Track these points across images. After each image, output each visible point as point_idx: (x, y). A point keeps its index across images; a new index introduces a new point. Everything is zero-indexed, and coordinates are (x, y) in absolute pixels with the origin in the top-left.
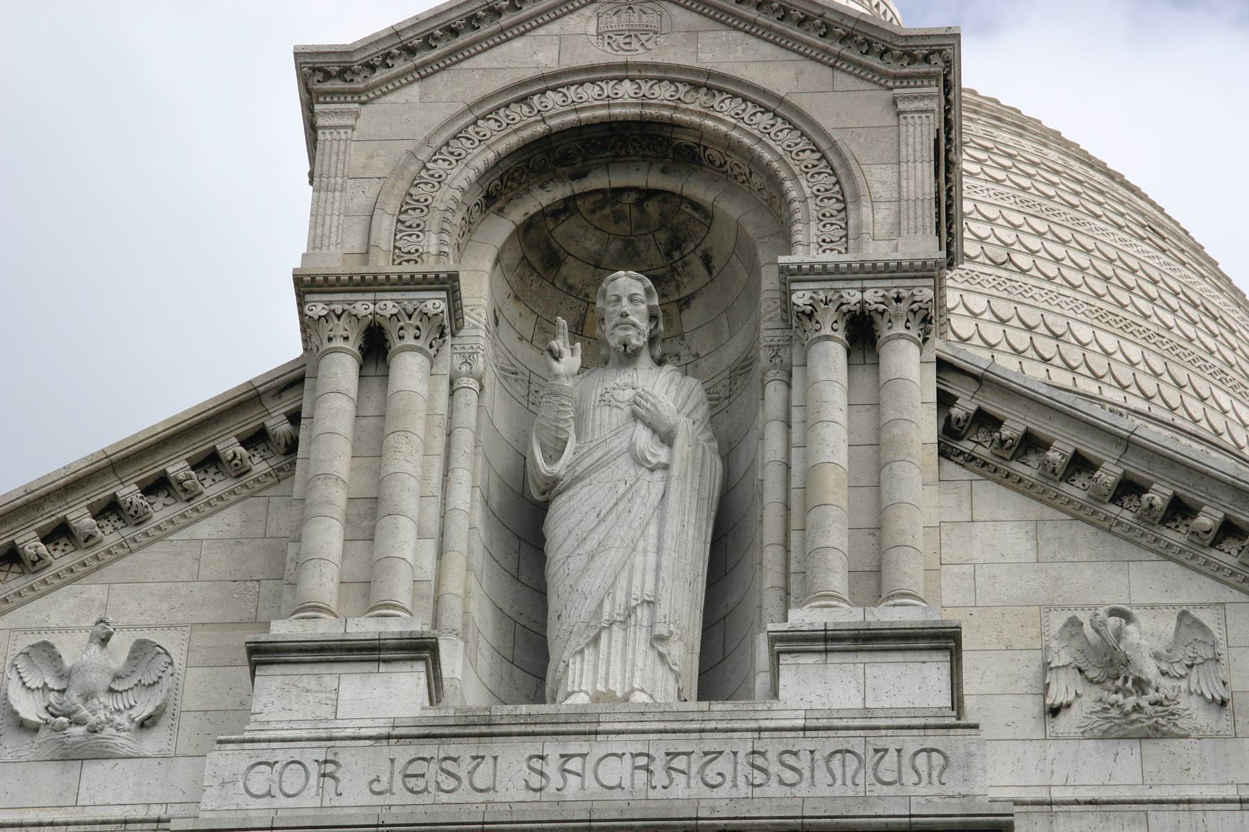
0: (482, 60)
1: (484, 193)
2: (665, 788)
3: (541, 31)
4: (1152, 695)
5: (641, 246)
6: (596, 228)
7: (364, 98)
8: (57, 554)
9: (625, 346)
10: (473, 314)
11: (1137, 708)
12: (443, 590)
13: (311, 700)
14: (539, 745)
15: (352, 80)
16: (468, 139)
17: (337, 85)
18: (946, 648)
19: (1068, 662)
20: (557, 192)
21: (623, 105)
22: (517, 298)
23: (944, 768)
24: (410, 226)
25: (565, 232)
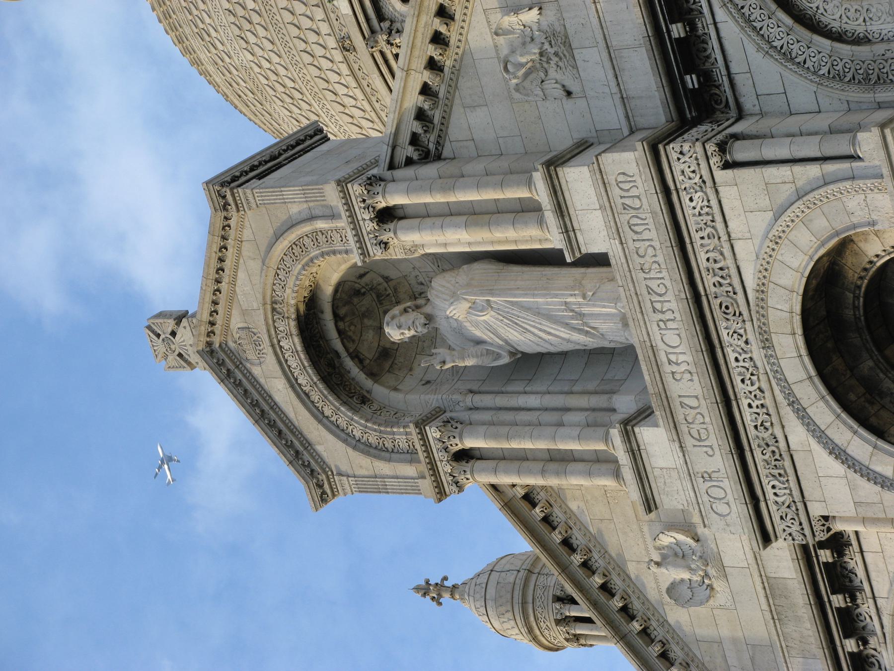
0: (292, 415)
1: (363, 405)
2: (673, 312)
3: (266, 387)
4: (547, 46)
5: (363, 309)
6: (361, 336)
7: (330, 473)
8: (617, 588)
9: (426, 324)
10: (430, 402)
11: (556, 54)
12: (587, 406)
13: (669, 480)
14: (667, 375)
15: (322, 480)
18: (556, 170)
19: (539, 89)
20: (349, 364)
21: (294, 345)
22: (411, 370)
23: (624, 174)
25: (368, 351)
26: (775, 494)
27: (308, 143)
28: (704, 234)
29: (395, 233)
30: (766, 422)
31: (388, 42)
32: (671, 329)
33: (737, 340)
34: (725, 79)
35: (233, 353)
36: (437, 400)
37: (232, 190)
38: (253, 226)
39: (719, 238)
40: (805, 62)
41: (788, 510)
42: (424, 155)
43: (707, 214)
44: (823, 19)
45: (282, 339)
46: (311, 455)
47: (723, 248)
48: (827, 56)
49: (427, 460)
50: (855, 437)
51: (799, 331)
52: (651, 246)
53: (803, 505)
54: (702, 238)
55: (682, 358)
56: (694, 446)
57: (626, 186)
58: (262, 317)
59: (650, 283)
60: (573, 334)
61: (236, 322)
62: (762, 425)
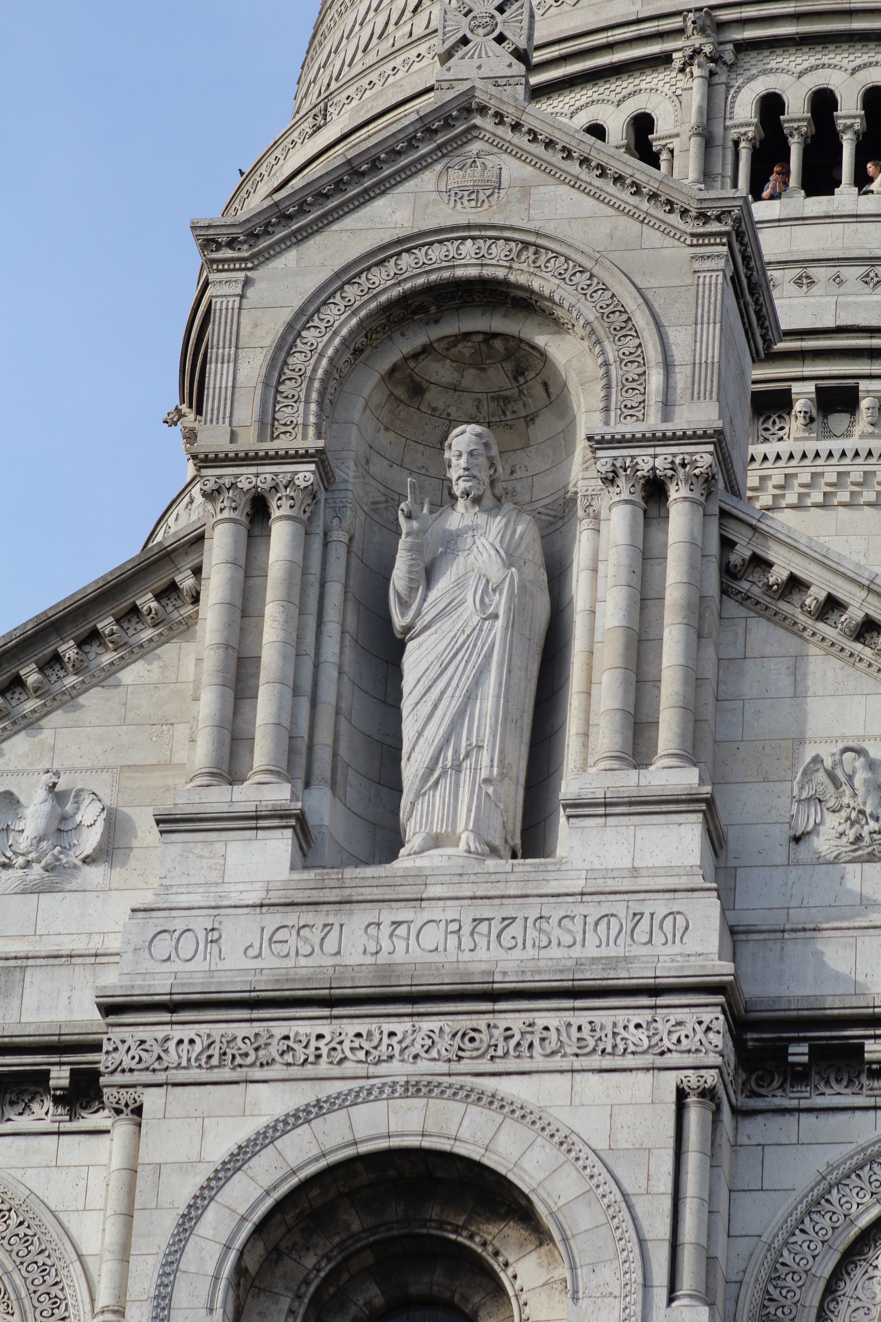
0: (349, 222)
2: (472, 950)
3: (400, 189)
7: (250, 265)
8: (14, 702)
10: (343, 468)
11: (859, 838)
16: (335, 304)
17: (227, 253)
21: (466, 265)
22: (387, 429)
23: (687, 928)
24: (286, 397)
26: (181, 1042)
27: (758, 332)
28: (586, 1032)
29: (626, 502)
30: (293, 1056)
31: (697, 52)
32: (446, 939)
33: (422, 1042)
34: (794, 1103)
35: (461, 146)
36: (346, 481)
37: (727, 234)
38: (664, 252)
39: (577, 1055)
40: (802, 1231)
41: (155, 1056)
42: (734, 571)
43: (615, 1046)
44: (859, 1271)
45: (476, 246)
46: (282, 240)
47: (563, 1056)
48: (808, 1267)
49: (261, 454)
50: (259, 1192)
51: (427, 1143)
52: (575, 943)
53: (160, 1082)
54: (580, 1028)
55: (400, 945)
56: (263, 929)
57: (668, 923)
58: (516, 222)
59: (519, 923)
60: (433, 748)
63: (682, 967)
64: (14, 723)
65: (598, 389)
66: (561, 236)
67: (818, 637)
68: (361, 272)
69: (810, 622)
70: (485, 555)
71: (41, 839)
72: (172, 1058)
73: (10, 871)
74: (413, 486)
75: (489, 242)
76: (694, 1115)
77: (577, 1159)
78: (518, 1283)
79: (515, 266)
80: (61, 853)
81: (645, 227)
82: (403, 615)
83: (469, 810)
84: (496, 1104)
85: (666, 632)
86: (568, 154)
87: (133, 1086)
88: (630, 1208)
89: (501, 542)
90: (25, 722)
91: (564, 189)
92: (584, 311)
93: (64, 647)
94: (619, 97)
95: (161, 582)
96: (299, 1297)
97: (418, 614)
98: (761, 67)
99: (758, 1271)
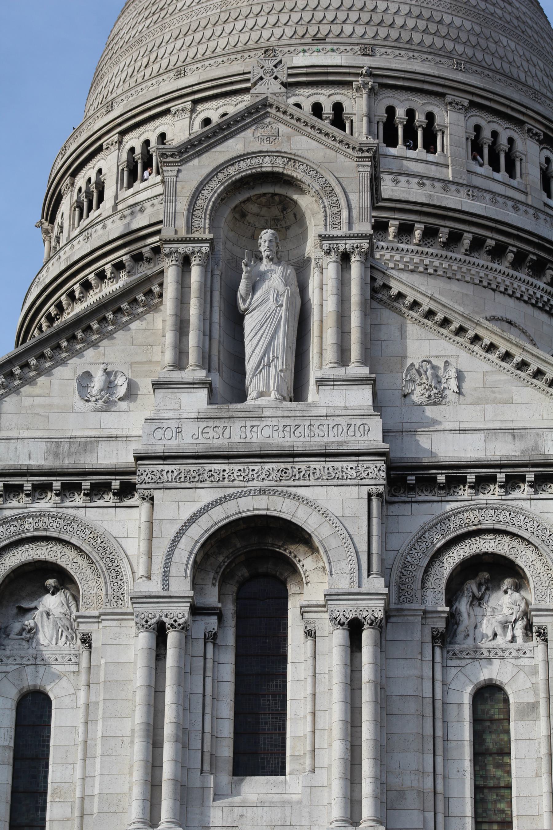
0: (219, 148)
3: (239, 136)
7: (179, 164)
11: (430, 396)
17: (171, 159)
21: (266, 167)
22: (232, 230)
23: (369, 430)
26: (168, 472)
28: (331, 470)
29: (335, 261)
36: (219, 251)
38: (345, 163)
39: (328, 479)
40: (415, 549)
43: (343, 476)
44: (437, 564)
49: (188, 239)
50: (203, 531)
51: (269, 513)
54: (328, 469)
55: (255, 435)
59: (302, 427)
61: (283, 129)
62: (212, 475)
63: (369, 445)
64: (88, 344)
65: (321, 216)
66: (304, 156)
67: (410, 317)
68: (225, 168)
69: (407, 311)
70: (277, 281)
71: (101, 390)
72: (165, 478)
73: (90, 403)
74: (248, 253)
75: (275, 158)
76: (375, 504)
77: (330, 520)
78: (305, 568)
79: (286, 167)
80: (109, 396)
81: (338, 154)
82: (244, 304)
83: (274, 382)
84: (296, 498)
85: (353, 314)
86: (306, 124)
87: (150, 489)
88: (352, 539)
89: (282, 276)
90: (92, 344)
91: (304, 138)
92: (314, 185)
93: (108, 314)
94: (235, 103)
95: (146, 289)
96: (217, 573)
97: (250, 304)
98: (292, 93)
99: (398, 564)
